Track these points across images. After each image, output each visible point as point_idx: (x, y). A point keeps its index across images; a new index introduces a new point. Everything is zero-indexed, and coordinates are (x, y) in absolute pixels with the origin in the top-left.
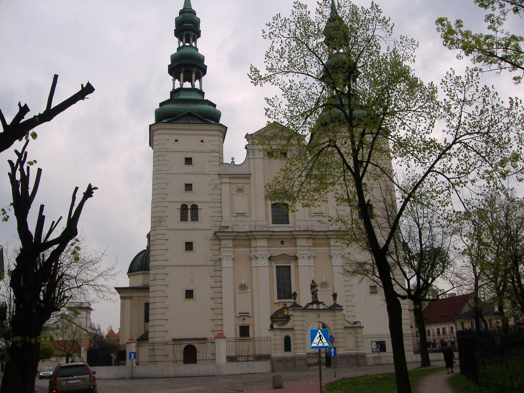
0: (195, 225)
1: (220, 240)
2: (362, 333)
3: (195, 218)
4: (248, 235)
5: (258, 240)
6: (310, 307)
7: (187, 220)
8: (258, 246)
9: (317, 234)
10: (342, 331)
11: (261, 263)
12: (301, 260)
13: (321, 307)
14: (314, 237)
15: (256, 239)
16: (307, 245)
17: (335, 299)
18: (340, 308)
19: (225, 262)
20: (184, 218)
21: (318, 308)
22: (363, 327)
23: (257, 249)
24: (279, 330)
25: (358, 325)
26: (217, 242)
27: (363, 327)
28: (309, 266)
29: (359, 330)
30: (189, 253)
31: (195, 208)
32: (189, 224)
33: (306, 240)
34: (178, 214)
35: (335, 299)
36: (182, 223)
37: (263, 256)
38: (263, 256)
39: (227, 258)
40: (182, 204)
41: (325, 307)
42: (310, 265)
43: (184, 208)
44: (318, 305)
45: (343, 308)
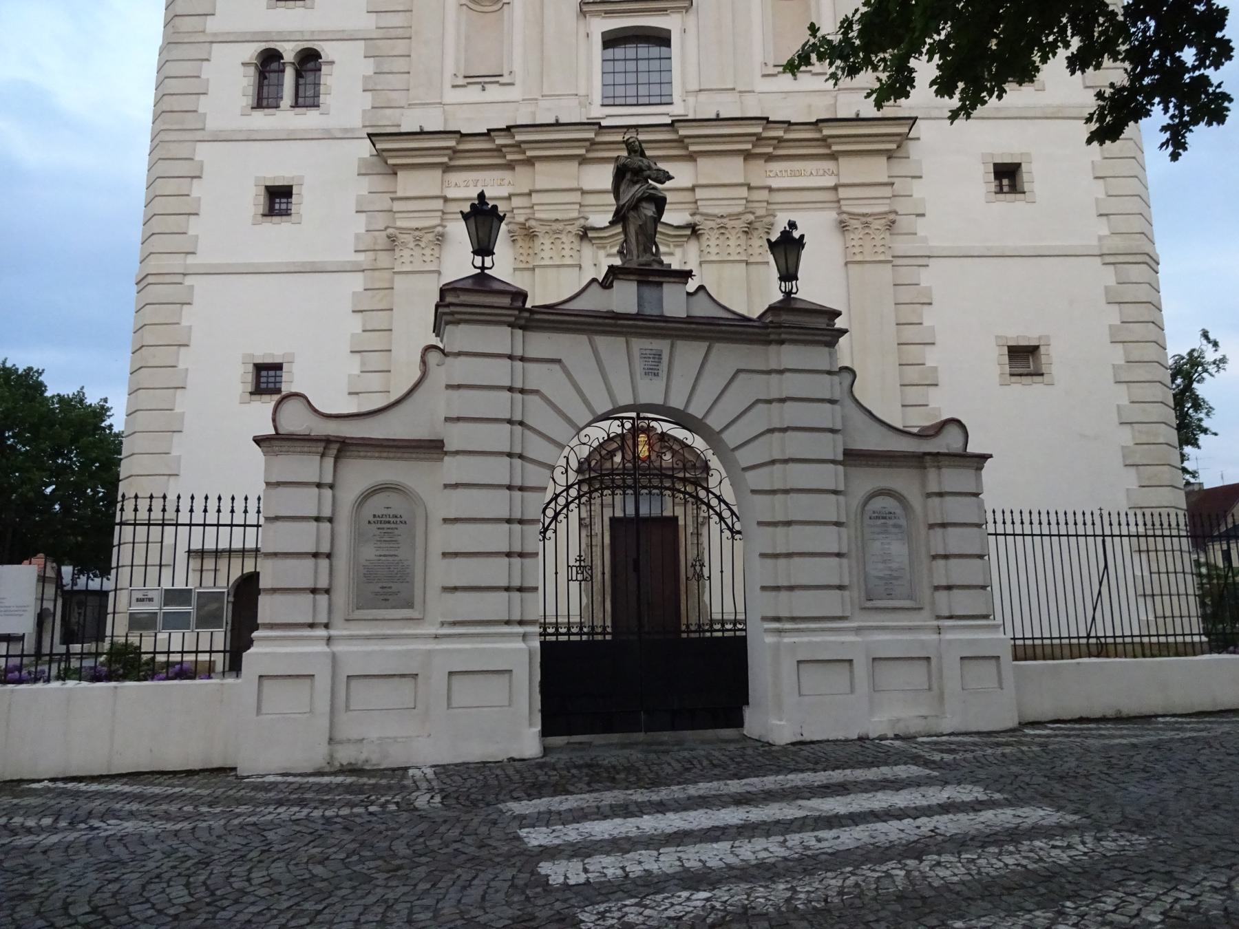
0: (309, 119)
1: (394, 171)
2: (976, 495)
3: (307, 99)
4: (499, 149)
5: (539, 166)
6: (597, 301)
7: (277, 107)
8: (538, 187)
9: (780, 133)
10: (829, 476)
11: (547, 254)
12: (713, 242)
13: (673, 302)
14: (770, 150)
15: (530, 162)
16: (742, 180)
17: (789, 275)
18: (821, 323)
19: (406, 253)
20: (264, 99)
21: (649, 310)
22: (985, 457)
23: (536, 198)
24: (306, 447)
25: (949, 442)
26: (381, 183)
27: (985, 457)
28: (747, 263)
29: (953, 479)
30: (278, 228)
31: (309, 60)
32: (285, 118)
33: (739, 161)
34: (245, 81)
35: (789, 275)
36: (259, 115)
37: (556, 226)
38: (556, 226)
39: (418, 240)
40: (264, 46)
41: (702, 309)
42: (752, 260)
43: (269, 61)
44: (649, 292)
45: (839, 323)
